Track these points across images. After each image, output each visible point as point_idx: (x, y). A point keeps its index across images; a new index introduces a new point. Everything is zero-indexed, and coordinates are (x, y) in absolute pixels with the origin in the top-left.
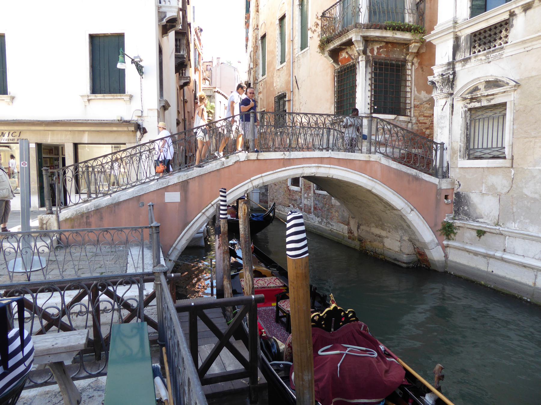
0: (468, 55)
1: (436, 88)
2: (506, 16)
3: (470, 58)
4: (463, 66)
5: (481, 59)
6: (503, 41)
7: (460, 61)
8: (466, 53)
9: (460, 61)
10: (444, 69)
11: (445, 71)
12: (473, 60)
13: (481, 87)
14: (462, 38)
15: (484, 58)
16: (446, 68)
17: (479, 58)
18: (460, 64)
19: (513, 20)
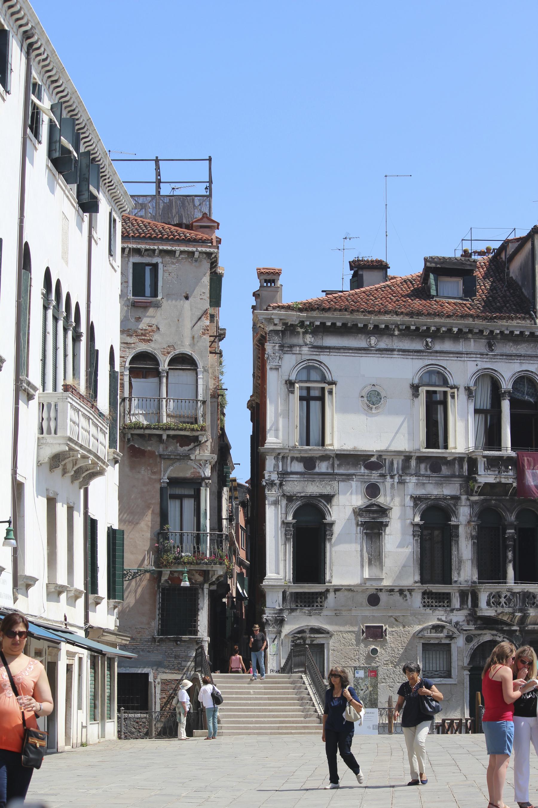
0: (293, 606)
1: (269, 624)
2: (323, 591)
3: (296, 609)
4: (290, 613)
5: (305, 612)
6: (319, 604)
7: (288, 609)
8: (291, 605)
9: (288, 609)
10: (275, 612)
11: (276, 614)
12: (298, 611)
13: (308, 631)
14: (288, 593)
15: (307, 612)
16: (278, 611)
17: (304, 611)
18: (287, 611)
19: (327, 594)
